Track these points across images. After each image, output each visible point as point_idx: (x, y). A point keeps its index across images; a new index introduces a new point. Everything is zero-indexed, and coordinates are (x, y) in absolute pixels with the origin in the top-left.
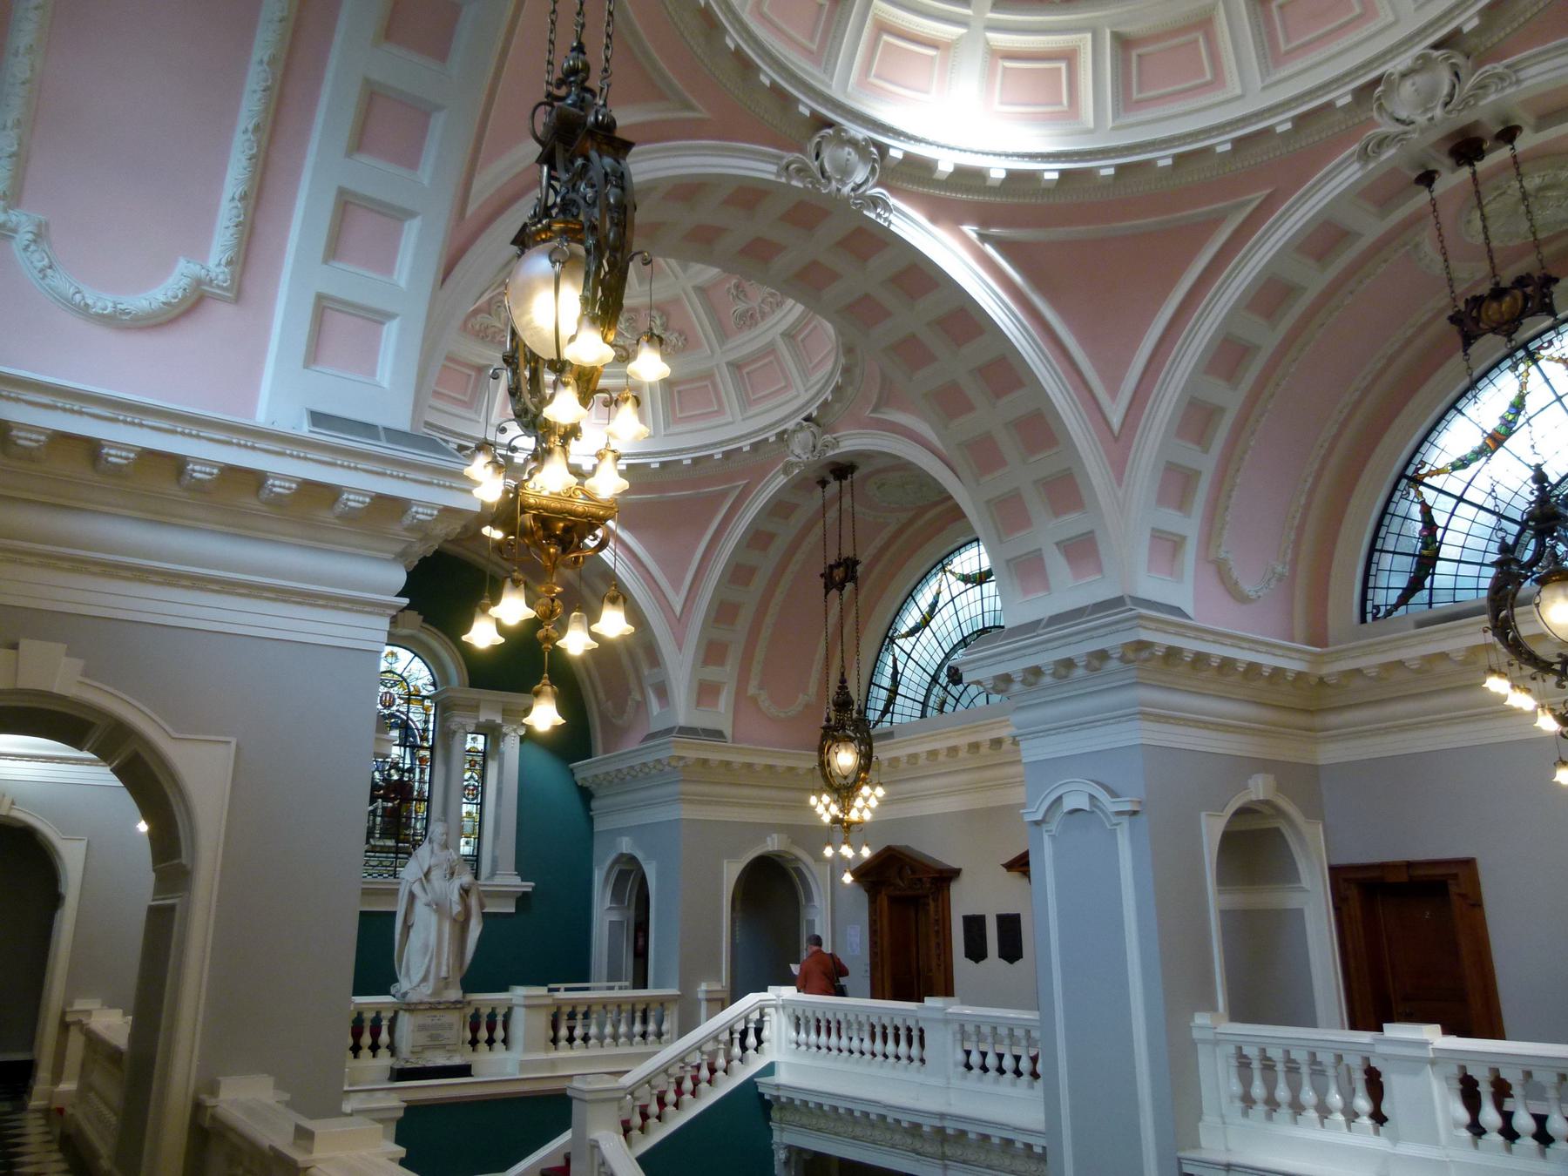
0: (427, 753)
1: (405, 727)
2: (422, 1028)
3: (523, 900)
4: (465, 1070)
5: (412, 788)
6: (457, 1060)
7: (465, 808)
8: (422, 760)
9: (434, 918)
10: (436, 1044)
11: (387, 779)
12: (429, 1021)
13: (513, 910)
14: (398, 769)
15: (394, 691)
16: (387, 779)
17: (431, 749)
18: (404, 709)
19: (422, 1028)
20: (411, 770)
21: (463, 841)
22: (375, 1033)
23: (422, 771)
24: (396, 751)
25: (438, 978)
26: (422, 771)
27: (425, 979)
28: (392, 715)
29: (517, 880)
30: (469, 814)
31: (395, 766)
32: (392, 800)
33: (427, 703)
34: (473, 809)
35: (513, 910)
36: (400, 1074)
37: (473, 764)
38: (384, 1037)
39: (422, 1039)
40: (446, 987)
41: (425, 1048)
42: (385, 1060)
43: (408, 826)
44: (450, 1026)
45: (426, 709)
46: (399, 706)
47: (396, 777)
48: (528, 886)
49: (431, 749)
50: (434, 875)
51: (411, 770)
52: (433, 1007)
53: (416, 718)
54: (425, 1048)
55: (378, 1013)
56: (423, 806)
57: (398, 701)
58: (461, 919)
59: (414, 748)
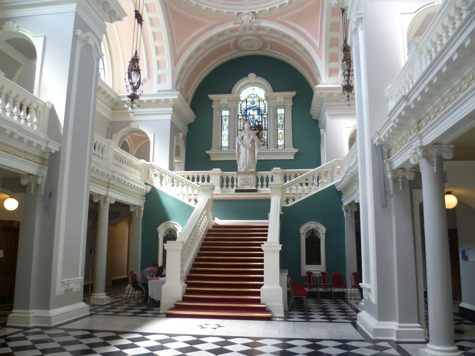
0: (266, 116)
1: (259, 110)
2: (242, 179)
3: (296, 155)
4: (256, 191)
5: (262, 127)
6: (254, 188)
7: (279, 131)
8: (265, 118)
9: (244, 149)
10: (247, 183)
11: (255, 125)
12: (244, 177)
13: (293, 158)
14: (257, 122)
15: (255, 100)
16: (255, 125)
17: (267, 115)
18: (258, 104)
19: (242, 179)
20: (262, 121)
21: (279, 141)
22: (233, 182)
23: (265, 121)
24: (256, 117)
25: (246, 166)
26: (265, 121)
27: (243, 166)
28: (255, 106)
29: (293, 149)
30: (281, 133)
31: (257, 121)
32: (257, 130)
33: (265, 101)
34: (282, 131)
35: (293, 158)
36: (237, 191)
37: (281, 118)
38: (235, 183)
39: (243, 182)
40: (250, 168)
41: (243, 185)
42: (235, 188)
43: (262, 138)
44: (251, 179)
45: (265, 104)
46: (257, 104)
47: (257, 124)
48: (296, 150)
49: (267, 115)
50: (245, 137)
51: (262, 121)
52: (245, 173)
53: (262, 106)
54: (243, 185)
55: (232, 177)
56: (266, 131)
57: (256, 102)
58: (252, 149)
59: (262, 115)
